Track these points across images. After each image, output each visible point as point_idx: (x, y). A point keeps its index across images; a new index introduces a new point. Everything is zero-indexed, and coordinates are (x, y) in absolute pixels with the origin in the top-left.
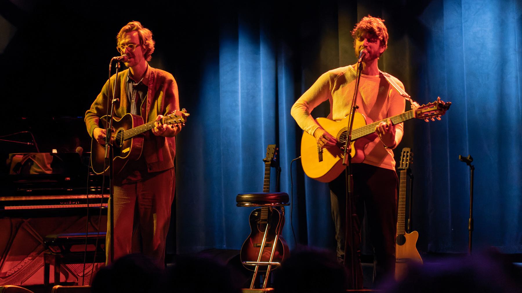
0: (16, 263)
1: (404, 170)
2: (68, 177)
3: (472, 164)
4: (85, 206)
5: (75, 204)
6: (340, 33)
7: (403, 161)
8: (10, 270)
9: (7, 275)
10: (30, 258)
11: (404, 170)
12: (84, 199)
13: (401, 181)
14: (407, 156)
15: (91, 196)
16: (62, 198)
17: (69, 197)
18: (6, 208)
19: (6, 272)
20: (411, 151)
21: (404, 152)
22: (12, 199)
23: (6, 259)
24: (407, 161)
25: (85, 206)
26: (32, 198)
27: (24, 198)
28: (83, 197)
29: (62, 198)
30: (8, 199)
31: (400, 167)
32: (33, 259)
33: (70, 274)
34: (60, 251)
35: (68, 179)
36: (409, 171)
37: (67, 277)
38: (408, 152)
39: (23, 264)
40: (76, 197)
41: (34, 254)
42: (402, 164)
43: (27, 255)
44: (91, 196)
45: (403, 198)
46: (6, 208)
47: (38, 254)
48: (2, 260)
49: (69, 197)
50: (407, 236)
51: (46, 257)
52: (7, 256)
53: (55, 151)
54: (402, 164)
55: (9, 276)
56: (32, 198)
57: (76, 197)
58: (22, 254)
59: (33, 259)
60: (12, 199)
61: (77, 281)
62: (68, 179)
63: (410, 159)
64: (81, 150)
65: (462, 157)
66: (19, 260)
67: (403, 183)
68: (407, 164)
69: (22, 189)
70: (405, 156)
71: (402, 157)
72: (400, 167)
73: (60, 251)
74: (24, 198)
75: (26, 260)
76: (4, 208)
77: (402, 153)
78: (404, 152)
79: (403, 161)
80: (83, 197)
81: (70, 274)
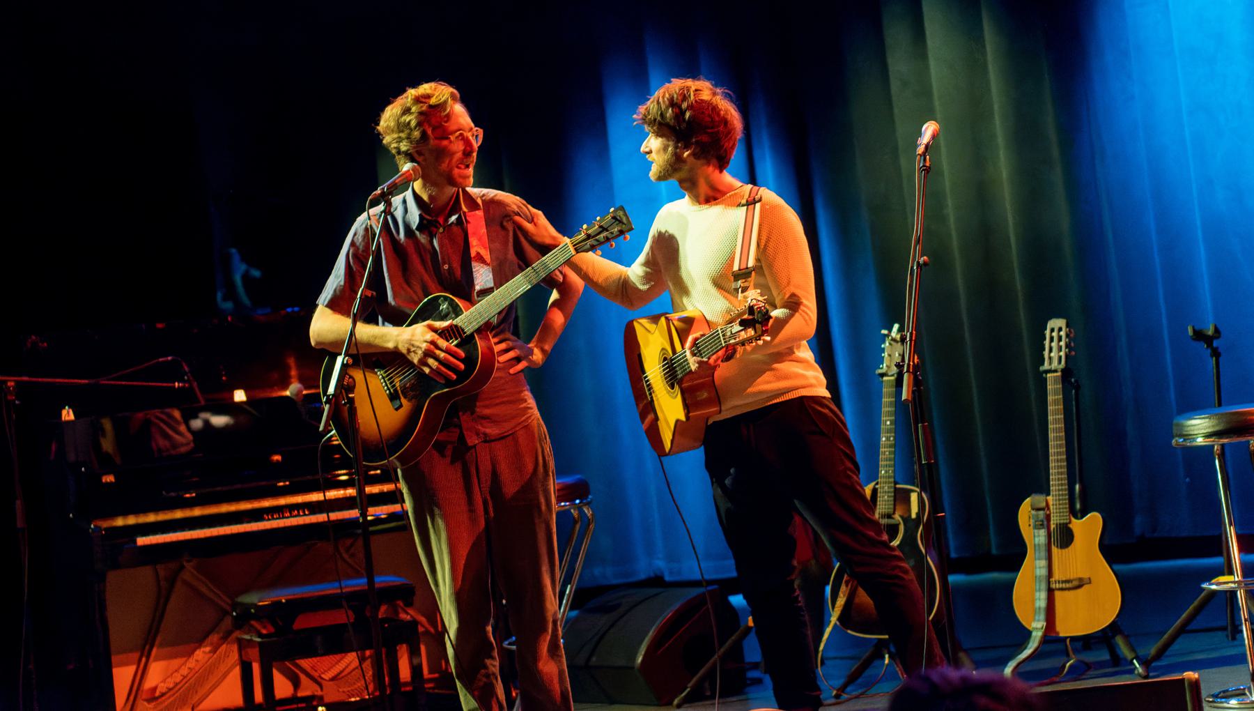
0: (176, 663)
1: (1055, 371)
2: (276, 453)
3: (1215, 343)
4: (321, 518)
5: (298, 515)
6: (889, 41)
7: (1051, 350)
8: (164, 681)
9: (157, 694)
10: (208, 649)
11: (1055, 371)
12: (318, 502)
13: (1050, 398)
14: (1060, 339)
15: (332, 494)
16: (267, 503)
17: (282, 501)
18: (142, 541)
19: (155, 689)
20: (1068, 326)
21: (1052, 330)
22: (151, 518)
23: (152, 658)
24: (1060, 349)
25: (321, 518)
26: (197, 512)
27: (179, 514)
28: (316, 497)
29: (267, 503)
31: (1046, 366)
32: (214, 651)
33: (302, 676)
34: (272, 630)
35: (277, 458)
36: (1066, 374)
37: (296, 684)
38: (1060, 329)
39: (191, 663)
40: (299, 499)
41: (214, 638)
42: (1050, 358)
43: (200, 643)
44: (332, 494)
45: (1056, 438)
46: (142, 541)
47: (225, 638)
48: (144, 660)
49: (282, 501)
50: (1077, 525)
51: (242, 645)
52: (154, 650)
53: (240, 396)
54: (1050, 358)
55: (163, 695)
56: (197, 512)
57: (299, 499)
58: (187, 641)
59: (214, 651)
60: (151, 518)
61: (319, 693)
62: (277, 458)
63: (1067, 346)
64: (300, 391)
65: (1194, 331)
66: (182, 656)
67: (1056, 402)
68: (1060, 358)
69: (173, 494)
70: (1056, 339)
71: (1047, 343)
72: (1046, 366)
73: (272, 630)
74: (179, 514)
75: (202, 654)
77: (1048, 332)
78: (1052, 330)
79: (1051, 350)
80: (316, 497)
81: (303, 677)
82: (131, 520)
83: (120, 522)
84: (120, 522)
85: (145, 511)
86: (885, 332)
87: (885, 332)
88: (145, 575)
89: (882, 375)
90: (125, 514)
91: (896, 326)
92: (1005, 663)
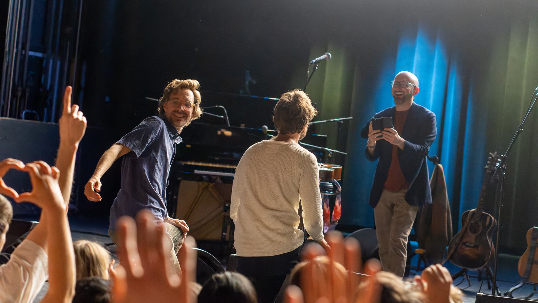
22: (200, 164)
26: (217, 166)
27: (210, 165)
30: (197, 164)
56: (217, 166)
60: (200, 164)
74: (210, 165)
76: (194, 172)
82: (193, 164)
83: (189, 163)
84: (189, 163)
85: (198, 161)
86: (491, 153)
87: (491, 153)
88: (194, 184)
89: (486, 169)
90: (191, 161)
91: (496, 153)
92: (510, 289)
